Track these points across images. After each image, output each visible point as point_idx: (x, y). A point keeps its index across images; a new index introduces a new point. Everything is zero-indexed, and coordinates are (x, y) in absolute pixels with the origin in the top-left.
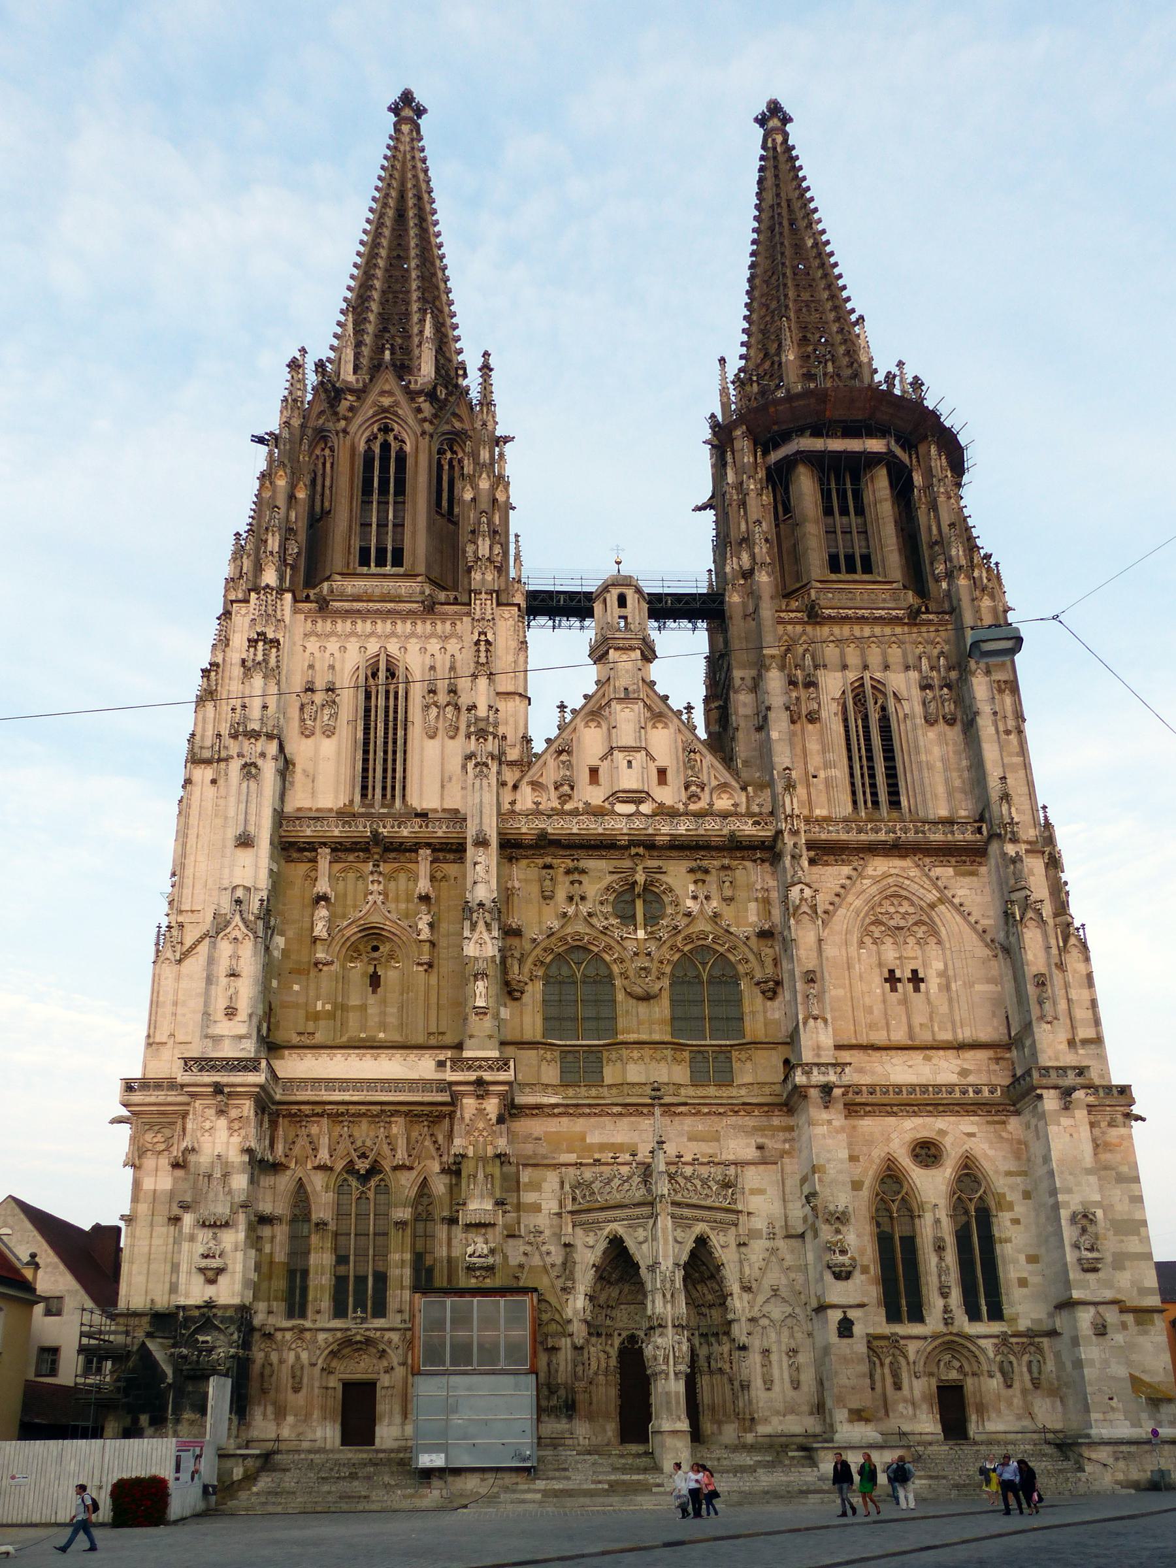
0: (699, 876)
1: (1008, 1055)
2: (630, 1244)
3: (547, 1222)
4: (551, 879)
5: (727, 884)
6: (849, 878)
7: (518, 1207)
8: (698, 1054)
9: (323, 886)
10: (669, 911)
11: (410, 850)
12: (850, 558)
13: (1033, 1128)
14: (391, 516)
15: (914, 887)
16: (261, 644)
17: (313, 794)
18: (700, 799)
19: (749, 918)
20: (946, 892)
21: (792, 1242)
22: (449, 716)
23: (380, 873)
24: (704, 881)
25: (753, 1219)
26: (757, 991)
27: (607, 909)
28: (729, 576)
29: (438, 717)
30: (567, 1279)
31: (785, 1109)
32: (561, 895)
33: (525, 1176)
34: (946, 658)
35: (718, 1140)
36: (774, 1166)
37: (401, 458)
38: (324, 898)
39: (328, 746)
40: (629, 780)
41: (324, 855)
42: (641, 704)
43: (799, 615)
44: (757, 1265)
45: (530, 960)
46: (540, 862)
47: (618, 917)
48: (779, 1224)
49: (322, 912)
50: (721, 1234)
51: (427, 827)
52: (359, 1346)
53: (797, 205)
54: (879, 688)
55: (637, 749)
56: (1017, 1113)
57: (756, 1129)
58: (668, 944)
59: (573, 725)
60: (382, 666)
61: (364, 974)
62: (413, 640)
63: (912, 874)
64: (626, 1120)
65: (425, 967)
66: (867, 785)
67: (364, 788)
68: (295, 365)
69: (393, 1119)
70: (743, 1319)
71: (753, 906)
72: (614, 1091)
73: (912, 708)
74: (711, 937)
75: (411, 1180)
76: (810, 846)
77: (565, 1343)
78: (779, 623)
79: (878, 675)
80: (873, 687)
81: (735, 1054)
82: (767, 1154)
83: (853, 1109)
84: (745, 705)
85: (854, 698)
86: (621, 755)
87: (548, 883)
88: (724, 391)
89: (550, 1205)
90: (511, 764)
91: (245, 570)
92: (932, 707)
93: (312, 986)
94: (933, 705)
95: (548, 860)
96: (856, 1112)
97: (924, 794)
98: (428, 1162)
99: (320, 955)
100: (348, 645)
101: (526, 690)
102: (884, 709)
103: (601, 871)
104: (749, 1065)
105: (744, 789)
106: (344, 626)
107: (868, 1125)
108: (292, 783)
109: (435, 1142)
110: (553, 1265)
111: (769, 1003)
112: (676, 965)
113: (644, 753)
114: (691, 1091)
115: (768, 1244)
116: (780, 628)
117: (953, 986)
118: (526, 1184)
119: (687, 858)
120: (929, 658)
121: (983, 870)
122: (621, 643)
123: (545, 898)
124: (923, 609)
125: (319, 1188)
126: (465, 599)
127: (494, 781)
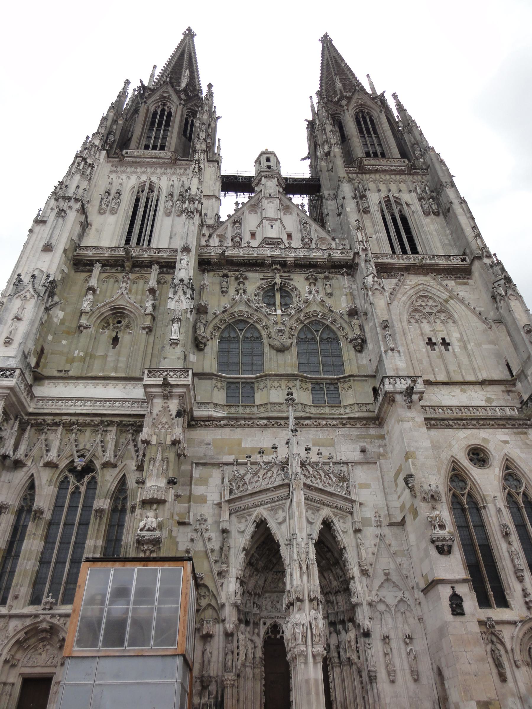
1: (514, 389)
2: (272, 525)
3: (211, 511)
4: (227, 282)
5: (328, 286)
7: (189, 499)
8: (317, 386)
9: (93, 282)
10: (295, 300)
15: (434, 291)
17: (99, 240)
21: (395, 529)
22: (178, 205)
23: (129, 278)
25: (364, 509)
26: (350, 346)
29: (172, 206)
30: (223, 563)
31: (377, 422)
33: (197, 473)
34: (429, 188)
35: (333, 446)
36: (374, 466)
37: (170, 114)
38: (92, 289)
39: (111, 219)
42: (278, 200)
43: (354, 169)
44: (371, 550)
45: (211, 326)
46: (221, 273)
48: (383, 513)
50: (341, 520)
52: (44, 635)
54: (398, 202)
55: (275, 219)
57: (360, 438)
59: (242, 210)
62: (164, 176)
64: (270, 430)
65: (147, 330)
69: (109, 429)
70: (365, 603)
71: (343, 298)
72: (262, 409)
74: (320, 314)
75: (114, 475)
77: (217, 630)
79: (396, 195)
80: (395, 201)
81: (340, 385)
82: (368, 456)
84: (331, 205)
86: (267, 222)
87: (225, 283)
89: (213, 497)
90: (208, 226)
92: (426, 207)
95: (225, 272)
97: (430, 246)
98: (128, 462)
100: (131, 177)
103: (256, 278)
104: (350, 391)
105: (334, 239)
108: (88, 234)
109: (135, 446)
110: (212, 551)
111: (359, 354)
113: (279, 221)
114: (313, 410)
115: (378, 531)
117: (468, 346)
118: (197, 480)
119: (304, 273)
121: (470, 282)
122: (267, 174)
123: (222, 292)
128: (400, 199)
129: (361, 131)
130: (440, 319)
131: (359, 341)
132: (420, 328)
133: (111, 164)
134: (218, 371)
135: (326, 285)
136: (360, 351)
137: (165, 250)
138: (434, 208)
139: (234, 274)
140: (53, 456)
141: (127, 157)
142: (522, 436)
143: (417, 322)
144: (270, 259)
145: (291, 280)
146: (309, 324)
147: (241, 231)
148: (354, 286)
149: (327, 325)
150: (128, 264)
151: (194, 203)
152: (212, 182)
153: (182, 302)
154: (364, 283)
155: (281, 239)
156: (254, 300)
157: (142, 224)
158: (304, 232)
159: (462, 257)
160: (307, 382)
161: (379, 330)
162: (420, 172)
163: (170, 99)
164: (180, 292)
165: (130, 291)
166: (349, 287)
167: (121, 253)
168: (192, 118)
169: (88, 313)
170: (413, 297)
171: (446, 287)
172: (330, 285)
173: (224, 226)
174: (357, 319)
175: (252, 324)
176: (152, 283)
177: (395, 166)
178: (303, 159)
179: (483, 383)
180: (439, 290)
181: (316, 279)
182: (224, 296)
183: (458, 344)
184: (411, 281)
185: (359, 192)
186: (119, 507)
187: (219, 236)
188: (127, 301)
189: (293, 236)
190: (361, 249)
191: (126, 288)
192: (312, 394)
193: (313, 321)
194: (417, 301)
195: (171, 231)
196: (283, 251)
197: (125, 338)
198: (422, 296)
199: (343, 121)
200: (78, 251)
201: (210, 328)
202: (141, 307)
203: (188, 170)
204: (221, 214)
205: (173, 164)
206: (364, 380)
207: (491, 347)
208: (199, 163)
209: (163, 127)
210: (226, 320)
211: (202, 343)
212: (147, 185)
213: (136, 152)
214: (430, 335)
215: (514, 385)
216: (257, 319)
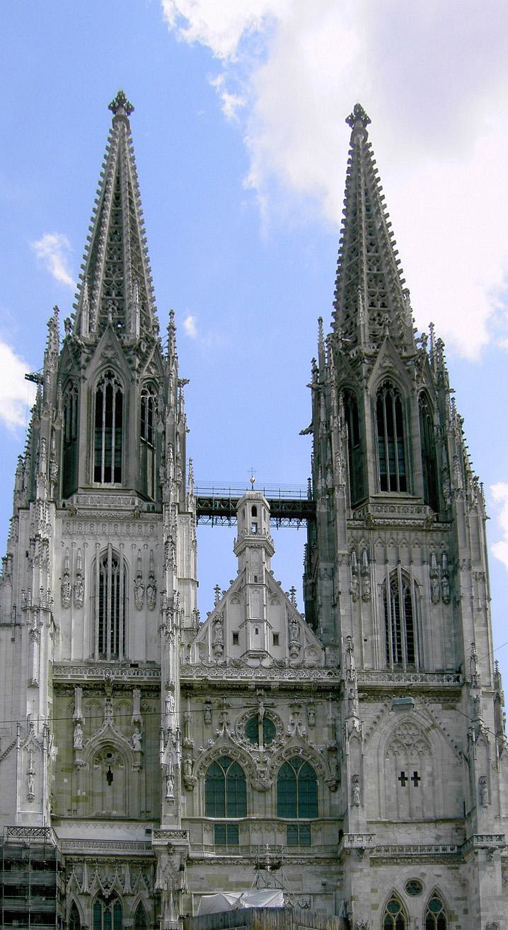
5: (312, 715)
6: (382, 711)
8: (292, 828)
9: (79, 714)
11: (128, 690)
12: (393, 478)
13: (472, 872)
14: (113, 444)
16: (37, 543)
19: (320, 741)
20: (436, 720)
22: (150, 595)
27: (242, 732)
28: (320, 493)
32: (216, 721)
35: (301, 880)
37: (119, 395)
38: (78, 721)
41: (79, 691)
43: (361, 523)
47: (249, 737)
49: (80, 732)
51: (138, 674)
54: (406, 577)
56: (465, 862)
57: (324, 874)
60: (110, 559)
61: (103, 772)
66: (396, 646)
67: (101, 645)
68: (52, 325)
71: (326, 729)
73: (424, 591)
74: (301, 751)
76: (360, 690)
78: (348, 528)
79: (406, 567)
80: (403, 576)
83: (375, 862)
85: (391, 584)
87: (208, 713)
88: (320, 345)
91: (25, 486)
93: (74, 780)
94: (437, 589)
95: (208, 698)
96: (377, 863)
98: (142, 892)
101: (195, 577)
102: (408, 591)
104: (320, 834)
106: (85, 528)
107: (383, 870)
109: (146, 880)
111: (333, 794)
112: (283, 768)
114: (287, 850)
116: (349, 532)
120: (436, 555)
121: (458, 705)
124: (435, 520)
125: (83, 906)
126: (159, 509)
127: (176, 643)
128: (409, 575)
131: (334, 782)
134: (208, 813)
135: (310, 714)
138: (445, 594)
140: (85, 888)
142: (453, 870)
146: (290, 761)
148: (338, 715)
150: (109, 690)
160: (283, 824)
173: (204, 629)
179: (437, 821)
183: (428, 779)
186: (141, 923)
187: (199, 644)
192: (287, 835)
194: (399, 729)
196: (268, 672)
197: (118, 774)
203: (155, 525)
206: (333, 824)
207: (457, 783)
211: (191, 785)
212: (110, 550)
215: (464, 823)
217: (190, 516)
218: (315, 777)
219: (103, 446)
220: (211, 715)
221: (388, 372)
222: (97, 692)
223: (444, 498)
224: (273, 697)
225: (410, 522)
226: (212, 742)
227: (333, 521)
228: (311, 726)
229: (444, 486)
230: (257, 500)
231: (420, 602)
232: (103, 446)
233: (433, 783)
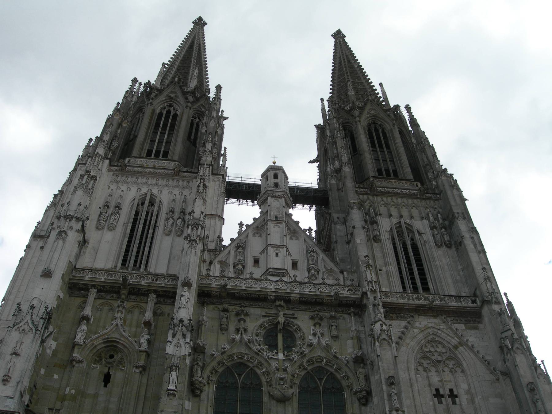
0: (317, 321)
4: (227, 318)
5: (334, 327)
9: (88, 311)
10: (299, 342)
12: (387, 171)
15: (444, 335)
18: (316, 278)
22: (179, 224)
23: (124, 307)
24: (320, 325)
29: (172, 224)
32: (232, 328)
34: (441, 215)
37: (175, 116)
39: (108, 236)
40: (276, 263)
41: (93, 293)
42: (284, 224)
46: (221, 307)
47: (266, 345)
49: (84, 327)
53: (350, 57)
54: (410, 228)
55: (282, 247)
58: (297, 364)
60: (148, 199)
63: (442, 327)
65: (141, 369)
71: (350, 342)
74: (325, 360)
79: (408, 221)
80: (407, 228)
87: (225, 319)
90: (209, 251)
92: (438, 237)
94: (438, 236)
95: (226, 306)
99: (76, 355)
100: (132, 188)
102: (412, 239)
105: (342, 272)
108: (85, 253)
111: (363, 408)
113: (285, 249)
121: (481, 326)
123: (222, 329)
126: (196, 171)
128: (412, 226)
129: (373, 145)
130: (448, 367)
131: (364, 393)
132: (428, 378)
133: (112, 173)
135: (332, 326)
136: (365, 404)
137: (163, 276)
138: (446, 239)
139: (235, 309)
141: (129, 166)
143: (425, 370)
144: (274, 294)
145: (296, 318)
146: (312, 372)
147: (244, 257)
148: (361, 329)
149: (331, 373)
150: (124, 292)
151: (197, 229)
152: (215, 199)
153: (180, 346)
154: (372, 330)
155: (287, 271)
156: (254, 341)
157: (140, 243)
158: (311, 262)
159: (473, 298)
161: (384, 387)
162: (433, 197)
163: (176, 100)
164: (179, 335)
165: (125, 321)
166: (355, 330)
167: (117, 278)
168: (197, 120)
169: (81, 345)
170: (422, 342)
171: (455, 332)
172: (336, 326)
173: (226, 251)
174: (363, 368)
175: (252, 369)
176: (148, 315)
177: (407, 189)
178: (311, 162)
180: (448, 335)
181: (321, 319)
182: (223, 334)
183: (466, 397)
184: (420, 324)
185: (369, 216)
188: (121, 333)
189: (299, 265)
190: (370, 290)
191: (121, 319)
193: (317, 367)
194: (426, 346)
195: (171, 253)
196: (288, 285)
197: (117, 376)
198: (432, 341)
199: (354, 132)
200: (74, 274)
201: (207, 372)
202: (135, 342)
203: (191, 182)
204: (223, 236)
205: (176, 176)
208: (204, 181)
209: (167, 131)
210: (224, 363)
211: (198, 389)
213: (139, 161)
214: (437, 385)
216: (257, 364)
217: (221, 177)
218: (340, 390)
219: (158, 138)
220: (228, 322)
221: (374, 116)
222: (112, 295)
223: (430, 181)
224: (292, 309)
225: (407, 191)
226: (227, 347)
227: (342, 188)
228: (335, 338)
229: (429, 174)
230: (279, 169)
231: (425, 245)
232: (158, 138)
233: (472, 401)
